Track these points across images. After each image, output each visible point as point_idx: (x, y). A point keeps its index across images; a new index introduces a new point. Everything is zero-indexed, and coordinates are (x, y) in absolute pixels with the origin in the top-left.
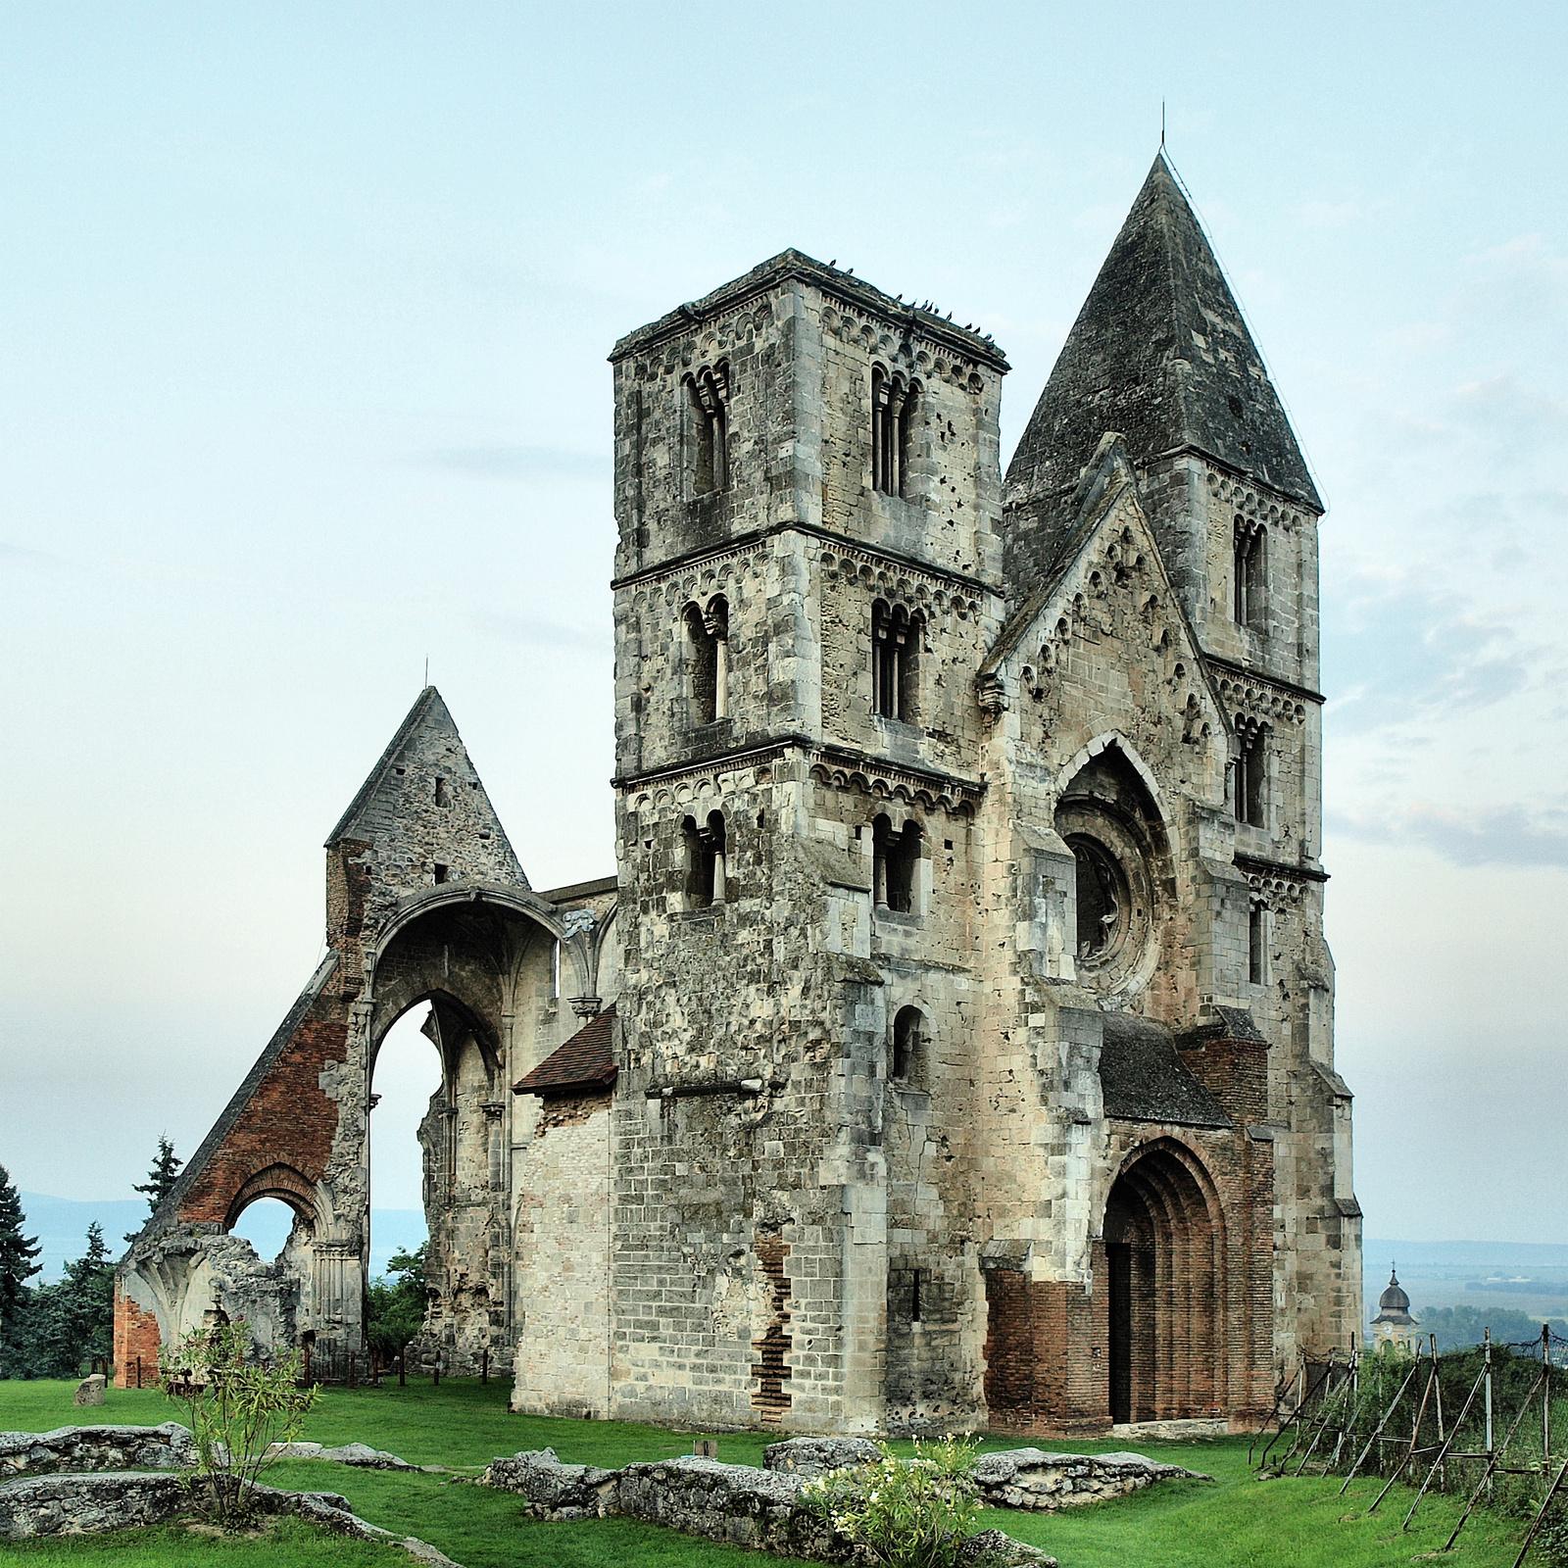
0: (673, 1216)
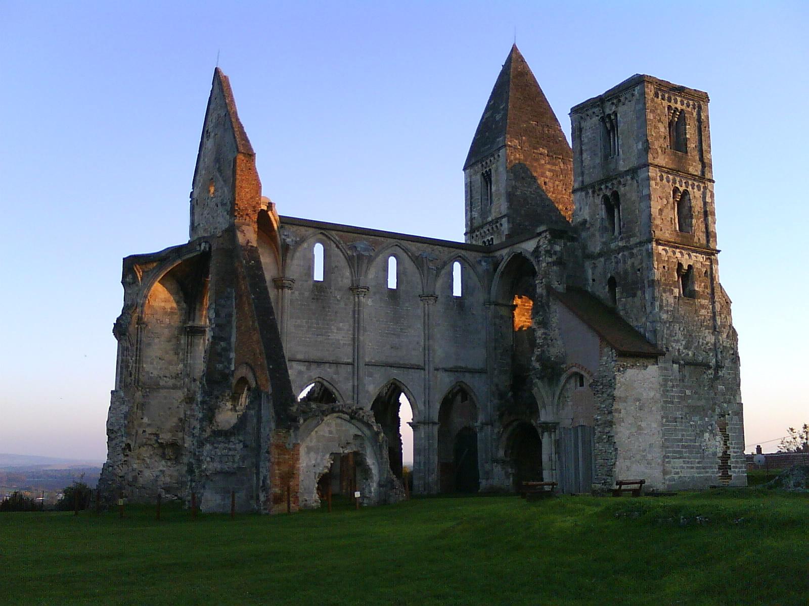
0: (686, 410)
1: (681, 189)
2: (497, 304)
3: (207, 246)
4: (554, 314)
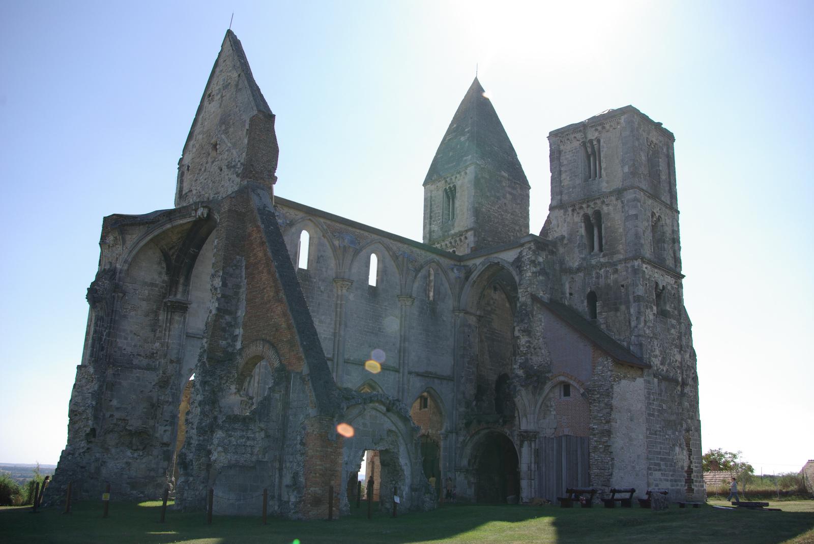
0: (662, 423)
1: (657, 215)
2: (467, 313)
3: (206, 212)
4: (539, 323)
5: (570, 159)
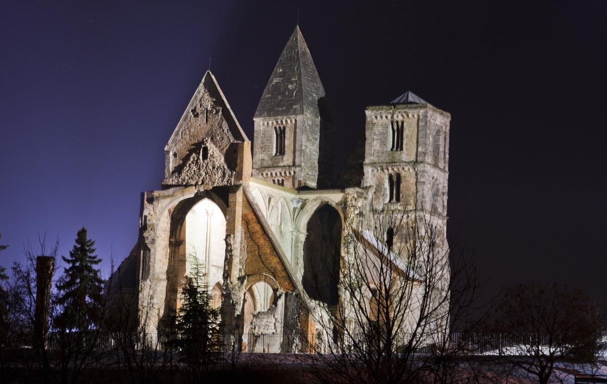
5: (381, 131)
